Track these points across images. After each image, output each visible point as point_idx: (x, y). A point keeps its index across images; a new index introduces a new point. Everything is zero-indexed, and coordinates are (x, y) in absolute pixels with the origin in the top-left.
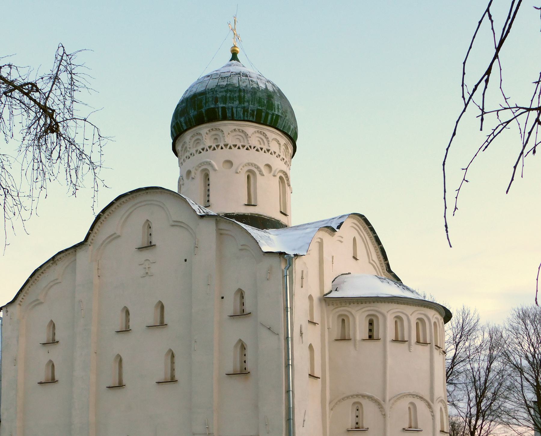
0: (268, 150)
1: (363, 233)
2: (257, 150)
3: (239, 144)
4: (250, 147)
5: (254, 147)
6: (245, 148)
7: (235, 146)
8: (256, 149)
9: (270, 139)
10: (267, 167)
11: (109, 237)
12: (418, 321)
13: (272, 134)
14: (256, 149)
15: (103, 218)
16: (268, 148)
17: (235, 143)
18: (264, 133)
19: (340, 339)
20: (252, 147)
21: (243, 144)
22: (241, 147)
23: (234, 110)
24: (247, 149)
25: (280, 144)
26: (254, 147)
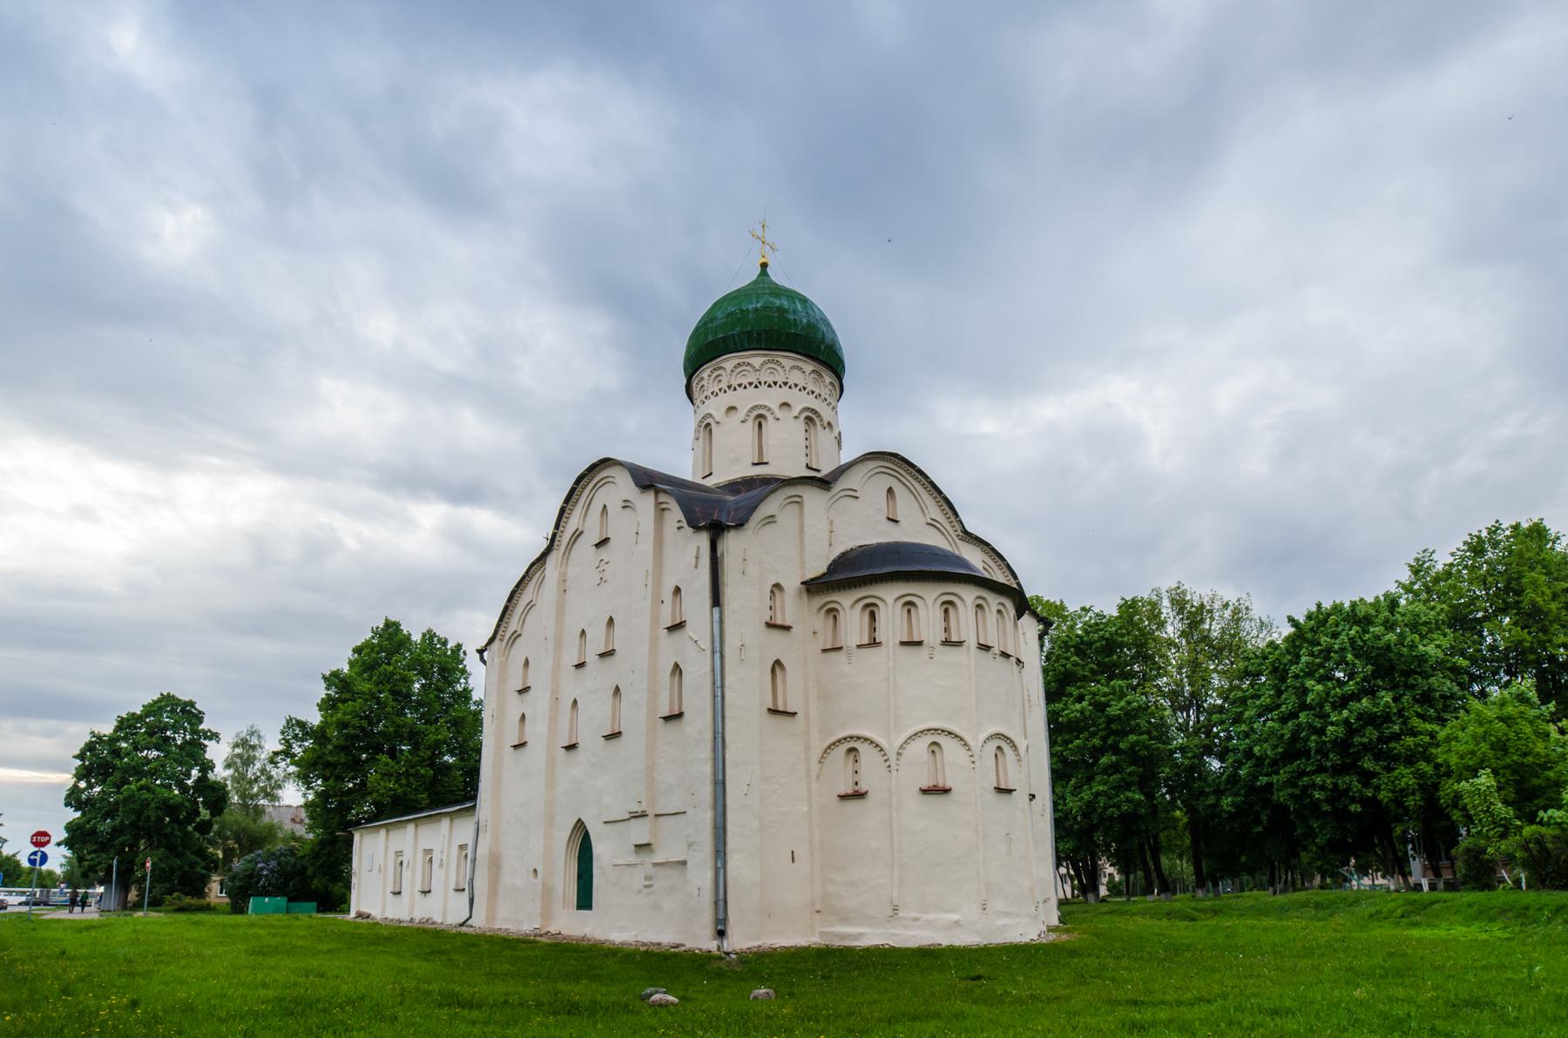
0: (785, 384)
1: (904, 477)
2: (770, 386)
3: (745, 382)
4: (760, 383)
5: (765, 383)
6: (754, 385)
7: (740, 385)
8: (767, 384)
9: (787, 368)
10: (785, 407)
11: (573, 535)
12: (946, 606)
13: (787, 360)
14: (767, 384)
15: (567, 511)
16: (786, 380)
17: (739, 382)
18: (778, 361)
19: (830, 647)
20: (763, 383)
21: (750, 381)
22: (748, 386)
23: (737, 338)
24: (756, 387)
25: (804, 372)
26: (765, 383)
